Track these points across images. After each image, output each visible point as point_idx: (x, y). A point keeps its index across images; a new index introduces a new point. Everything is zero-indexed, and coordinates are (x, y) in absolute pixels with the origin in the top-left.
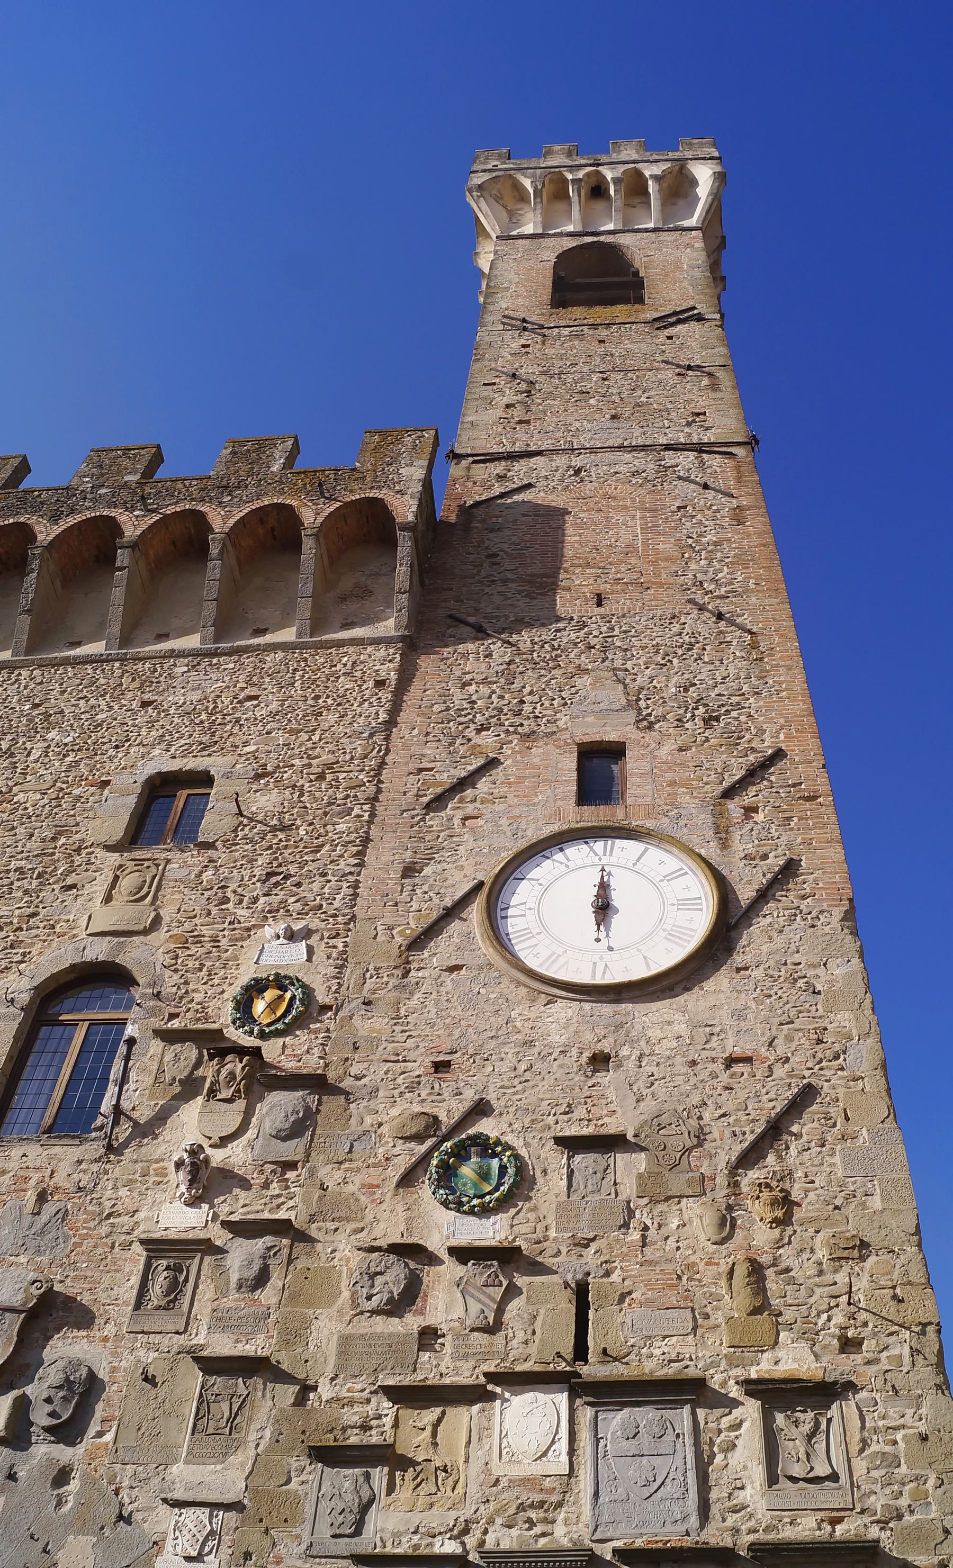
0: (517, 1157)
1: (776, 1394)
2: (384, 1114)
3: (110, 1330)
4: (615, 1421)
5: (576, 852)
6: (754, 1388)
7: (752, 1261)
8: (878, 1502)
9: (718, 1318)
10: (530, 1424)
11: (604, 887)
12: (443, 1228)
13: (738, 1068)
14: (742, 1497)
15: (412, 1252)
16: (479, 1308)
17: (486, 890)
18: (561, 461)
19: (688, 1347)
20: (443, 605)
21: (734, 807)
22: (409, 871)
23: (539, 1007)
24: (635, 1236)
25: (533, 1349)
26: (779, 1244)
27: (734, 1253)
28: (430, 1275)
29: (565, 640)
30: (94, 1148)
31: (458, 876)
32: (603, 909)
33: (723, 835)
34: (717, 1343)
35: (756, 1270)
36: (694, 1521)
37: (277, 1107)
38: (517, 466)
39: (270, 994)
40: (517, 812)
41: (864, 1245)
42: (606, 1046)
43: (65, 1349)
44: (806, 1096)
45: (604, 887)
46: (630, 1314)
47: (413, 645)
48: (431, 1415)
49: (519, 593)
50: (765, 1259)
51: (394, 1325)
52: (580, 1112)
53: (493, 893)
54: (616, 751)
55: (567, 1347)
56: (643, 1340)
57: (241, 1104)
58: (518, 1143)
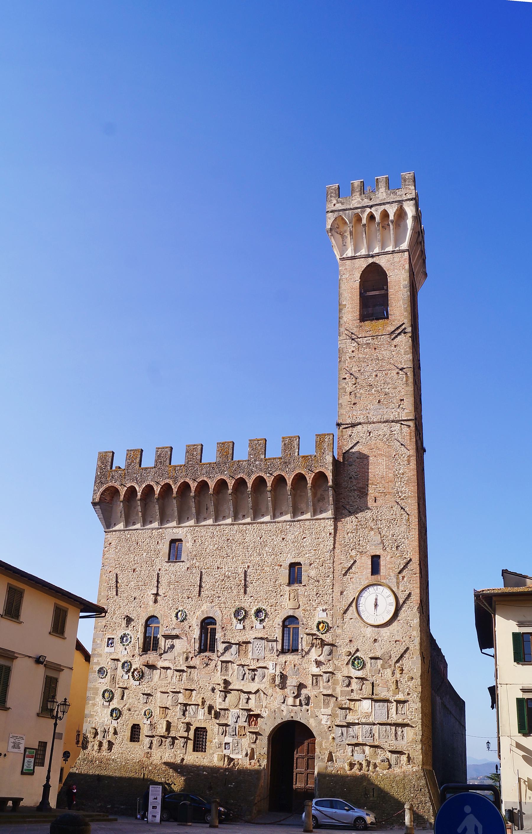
0: (363, 660)
1: (398, 702)
2: (343, 650)
3: (309, 689)
4: (377, 704)
5: (371, 589)
7: (396, 680)
8: (409, 718)
9: (391, 689)
10: (366, 704)
11: (376, 599)
13: (397, 642)
14: (393, 716)
16: (359, 687)
19: (387, 693)
21: (400, 576)
22: (342, 593)
23: (365, 628)
24: (380, 675)
26: (400, 677)
28: (352, 680)
30: (300, 657)
32: (376, 605)
33: (398, 583)
34: (391, 693)
35: (397, 681)
37: (327, 648)
38: (355, 430)
39: (322, 625)
40: (360, 577)
41: (412, 678)
42: (376, 638)
43: (304, 692)
44: (408, 649)
45: (376, 599)
46: (379, 688)
47: (336, 519)
48: (354, 702)
49: (358, 495)
50: (398, 680)
51: (347, 689)
52: (372, 651)
53: (356, 600)
54: (378, 557)
55: (371, 694)
57: (321, 648)
58: (363, 657)
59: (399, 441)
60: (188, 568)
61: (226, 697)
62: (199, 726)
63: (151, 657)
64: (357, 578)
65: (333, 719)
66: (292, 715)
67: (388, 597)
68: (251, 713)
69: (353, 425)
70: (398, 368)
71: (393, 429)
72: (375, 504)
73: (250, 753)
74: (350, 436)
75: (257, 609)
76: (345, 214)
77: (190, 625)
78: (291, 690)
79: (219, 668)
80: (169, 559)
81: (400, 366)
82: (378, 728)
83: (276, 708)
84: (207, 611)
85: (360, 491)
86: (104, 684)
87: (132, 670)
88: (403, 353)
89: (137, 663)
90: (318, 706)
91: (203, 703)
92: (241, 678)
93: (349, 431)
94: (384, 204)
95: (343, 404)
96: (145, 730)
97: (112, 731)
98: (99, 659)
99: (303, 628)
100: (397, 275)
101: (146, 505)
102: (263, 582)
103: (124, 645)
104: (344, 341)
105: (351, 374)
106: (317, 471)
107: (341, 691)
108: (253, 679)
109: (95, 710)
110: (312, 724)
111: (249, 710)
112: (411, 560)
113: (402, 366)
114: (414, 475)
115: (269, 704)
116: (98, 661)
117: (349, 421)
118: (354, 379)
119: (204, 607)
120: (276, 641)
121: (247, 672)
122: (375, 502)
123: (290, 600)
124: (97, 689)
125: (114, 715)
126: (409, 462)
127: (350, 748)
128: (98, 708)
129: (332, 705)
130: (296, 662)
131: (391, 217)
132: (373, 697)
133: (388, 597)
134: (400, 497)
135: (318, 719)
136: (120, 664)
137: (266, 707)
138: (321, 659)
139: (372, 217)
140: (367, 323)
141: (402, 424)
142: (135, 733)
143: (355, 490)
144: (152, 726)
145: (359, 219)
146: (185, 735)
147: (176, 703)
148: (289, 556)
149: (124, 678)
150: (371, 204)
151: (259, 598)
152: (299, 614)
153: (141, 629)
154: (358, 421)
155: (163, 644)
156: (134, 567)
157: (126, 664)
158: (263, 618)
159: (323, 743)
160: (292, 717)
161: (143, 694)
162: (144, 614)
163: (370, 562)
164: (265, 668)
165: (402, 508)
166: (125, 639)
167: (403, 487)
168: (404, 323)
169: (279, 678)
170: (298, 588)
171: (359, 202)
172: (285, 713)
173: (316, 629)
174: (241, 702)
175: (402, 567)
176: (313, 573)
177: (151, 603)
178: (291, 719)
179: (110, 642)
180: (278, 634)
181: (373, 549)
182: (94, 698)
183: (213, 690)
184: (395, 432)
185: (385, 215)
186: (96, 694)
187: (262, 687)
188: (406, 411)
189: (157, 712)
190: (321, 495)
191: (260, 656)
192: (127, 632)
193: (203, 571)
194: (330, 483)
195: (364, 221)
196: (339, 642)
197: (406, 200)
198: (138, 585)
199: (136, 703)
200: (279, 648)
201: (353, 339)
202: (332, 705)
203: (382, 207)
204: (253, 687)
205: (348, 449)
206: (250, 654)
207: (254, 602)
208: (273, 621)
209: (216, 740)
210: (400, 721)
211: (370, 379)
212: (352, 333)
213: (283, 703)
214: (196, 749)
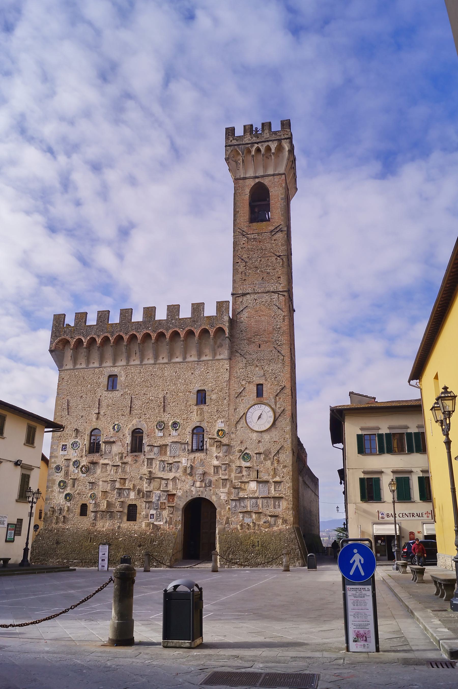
6: (273, 482)
10: (253, 485)
12: (244, 464)
13: (275, 443)
18: (253, 296)
22: (235, 409)
27: (273, 467)
33: (276, 403)
34: (271, 477)
38: (245, 298)
39: (221, 432)
51: (239, 475)
54: (262, 385)
59: (277, 306)
61: (150, 482)
62: (131, 503)
63: (95, 457)
64: (246, 399)
66: (199, 493)
67: (268, 412)
68: (170, 493)
69: (244, 295)
70: (276, 255)
71: (273, 297)
72: (259, 349)
74: (242, 302)
76: (239, 148)
79: (146, 463)
80: (107, 389)
81: (278, 254)
82: (261, 500)
83: (187, 489)
85: (248, 340)
86: (59, 477)
88: (280, 245)
89: (84, 462)
90: (217, 487)
92: (162, 469)
94: (268, 141)
95: (236, 280)
96: (91, 508)
97: (66, 508)
98: (56, 459)
99: (207, 434)
103: (74, 449)
105: (242, 259)
106: (218, 327)
108: (171, 470)
109: (53, 495)
110: (214, 499)
111: (168, 491)
112: (285, 386)
113: (279, 254)
114: (287, 329)
117: (240, 292)
118: (244, 263)
119: (134, 422)
120: (187, 443)
121: (166, 465)
123: (197, 415)
124: (55, 480)
125: (68, 498)
126: (284, 320)
127: (241, 515)
128: (56, 494)
129: (228, 486)
131: (273, 151)
133: (268, 412)
135: (219, 496)
136: (71, 463)
137: (180, 489)
138: (221, 454)
139: (258, 150)
140: (254, 224)
141: (279, 294)
142: (84, 510)
143: (244, 339)
144: (96, 505)
145: (249, 152)
146: (121, 510)
147: (114, 489)
149: (74, 472)
150: (258, 141)
152: (204, 425)
153: (87, 438)
154: (247, 292)
155: (104, 448)
156: (82, 395)
159: (222, 512)
160: (199, 495)
161: (89, 483)
162: (89, 428)
163: (255, 389)
164: (179, 462)
165: (279, 352)
166: (75, 445)
167: (279, 337)
170: (203, 407)
171: (249, 140)
173: (216, 435)
174: (162, 486)
176: (214, 397)
177: (94, 420)
178: (199, 496)
179: (64, 448)
180: (188, 438)
181: (258, 380)
182: (52, 487)
183: (141, 478)
184: (274, 300)
185: (268, 149)
186: (54, 484)
187: (177, 475)
188: (282, 285)
191: (176, 454)
192: (76, 440)
193: (133, 396)
194: (227, 335)
195: (253, 153)
196: (233, 443)
197: (284, 139)
200: (190, 448)
201: (243, 235)
202: (228, 486)
203: (267, 144)
204: (171, 475)
206: (169, 453)
209: (144, 513)
210: (277, 495)
213: (193, 486)
214: (128, 520)
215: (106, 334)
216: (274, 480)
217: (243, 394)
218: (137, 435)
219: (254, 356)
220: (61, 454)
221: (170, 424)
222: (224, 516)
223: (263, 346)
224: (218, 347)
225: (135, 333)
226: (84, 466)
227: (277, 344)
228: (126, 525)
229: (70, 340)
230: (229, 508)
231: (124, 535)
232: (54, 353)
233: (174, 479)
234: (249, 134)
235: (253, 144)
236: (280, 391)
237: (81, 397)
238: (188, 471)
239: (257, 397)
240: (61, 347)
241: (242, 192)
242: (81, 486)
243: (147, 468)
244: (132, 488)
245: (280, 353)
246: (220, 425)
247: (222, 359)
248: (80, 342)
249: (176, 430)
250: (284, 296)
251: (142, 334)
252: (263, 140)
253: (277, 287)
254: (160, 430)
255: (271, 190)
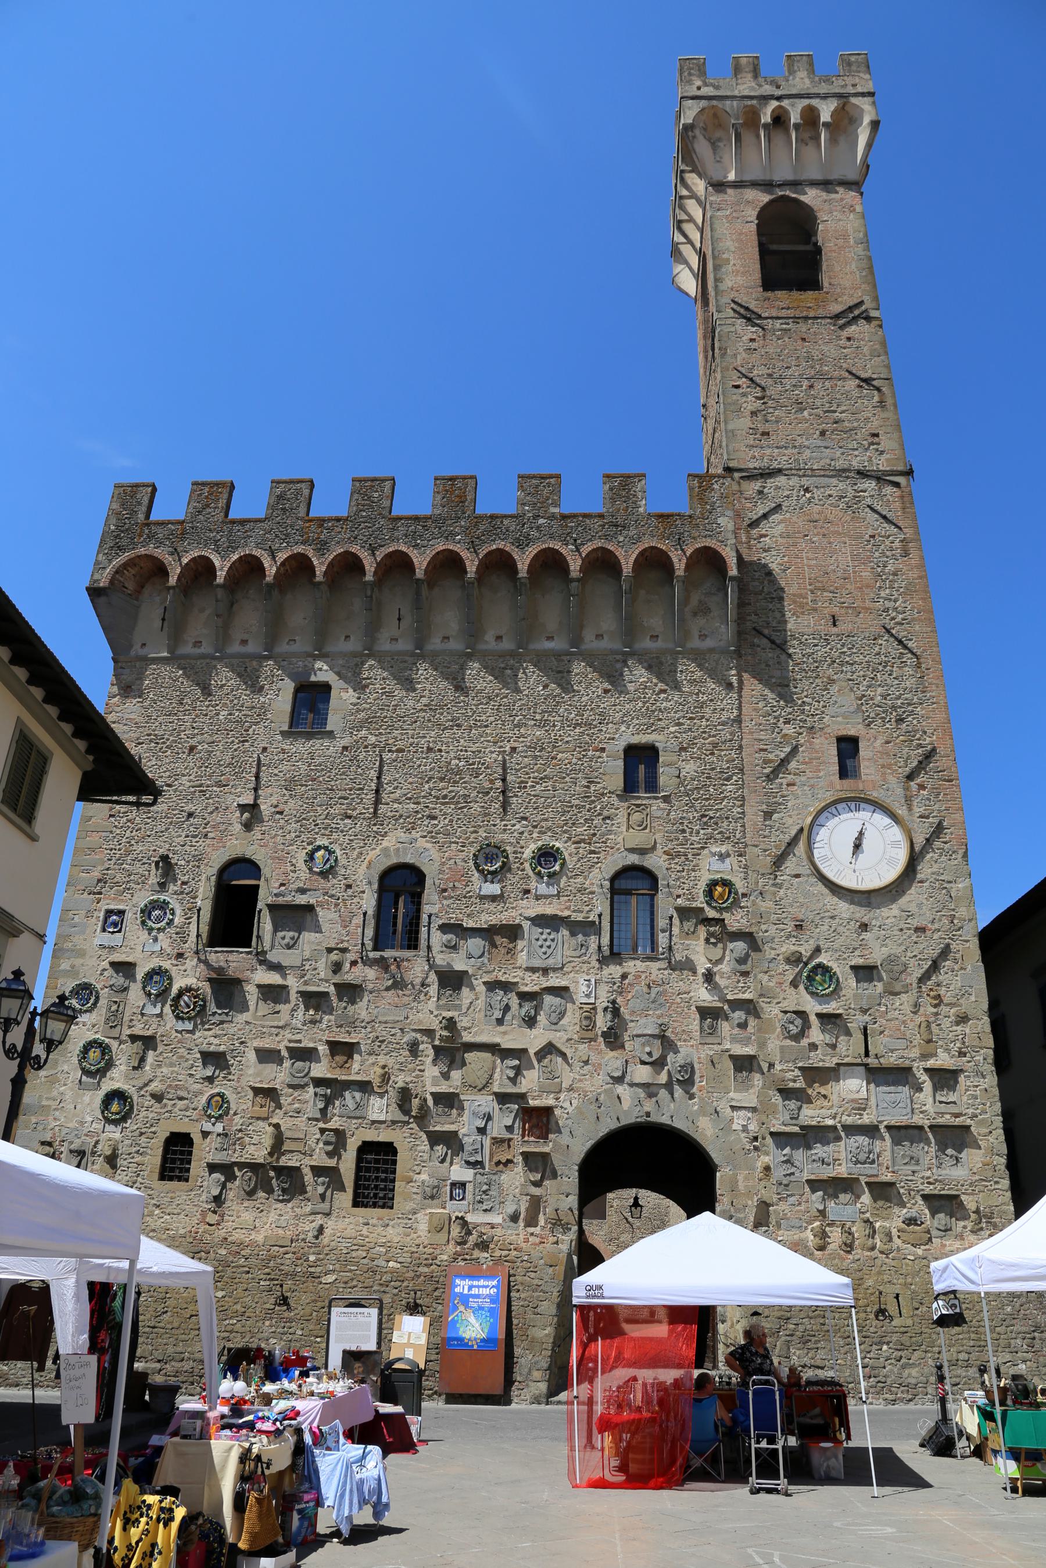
8: (970, 1111)
9: (915, 1042)
12: (812, 1007)
15: (802, 1014)
17: (805, 832)
18: (794, 481)
20: (749, 618)
22: (768, 815)
25: (850, 1052)
29: (820, 653)
31: (790, 821)
32: (857, 846)
33: (908, 800)
34: (915, 1053)
36: (909, 1116)
38: (770, 482)
40: (812, 782)
42: (865, 920)
46: (884, 1039)
56: (889, 1051)
60: (345, 748)
63: (233, 960)
65: (764, 1118)
70: (858, 378)
71: (862, 487)
72: (835, 630)
73: (527, 1210)
74: (760, 492)
75: (540, 849)
77: (350, 882)
78: (643, 1045)
80: (291, 727)
84: (398, 849)
87: (174, 991)
89: (188, 976)
91: (385, 1078)
93: (756, 485)
94: (808, 96)
96: (205, 1152)
98: (78, 962)
100: (840, 220)
101: (232, 605)
102: (554, 787)
103: (151, 930)
104: (729, 321)
107: (782, 1047)
109: (55, 1093)
110: (705, 1131)
111: (522, 1097)
112: (934, 750)
115: (581, 1080)
116: (73, 966)
121: (514, 1001)
122: (835, 625)
123: (629, 827)
125: (115, 1107)
126: (906, 553)
130: (653, 977)
132: (869, 1060)
134: (893, 619)
137: (571, 1089)
139: (779, 120)
148: (623, 728)
151: (543, 824)
152: (656, 862)
154: (775, 465)
157: (156, 978)
158: (557, 868)
159: (740, 1178)
160: (648, 1114)
163: (834, 751)
164: (566, 989)
168: (862, 303)
169: (609, 1016)
172: (626, 1104)
173: (702, 899)
174: (496, 1076)
175: (915, 763)
176: (689, 768)
177: (238, 827)
179: (114, 920)
181: (840, 723)
184: (866, 494)
185: (811, 117)
187: (559, 1039)
188: (885, 456)
189: (242, 1104)
190: (700, 601)
192: (162, 898)
193: (387, 756)
196: (767, 931)
198: (201, 785)
199: (180, 1077)
204: (533, 1040)
205: (755, 517)
207: (531, 833)
208: (585, 879)
209: (424, 1177)
211: (797, 392)
212: (747, 309)
215: (299, 549)
216: (931, 1063)
217: (793, 765)
218: (402, 884)
219: (821, 652)
220: (97, 941)
221: (528, 853)
222: (749, 1194)
223: (843, 627)
224: (695, 614)
225: (404, 549)
226: (189, 989)
227: (893, 619)
228: (347, 1224)
229: (168, 560)
230: (767, 1169)
231: (345, 1261)
232: (102, 600)
233: (549, 1049)
234: (750, 76)
235: (765, 99)
236: (920, 762)
237: (192, 749)
238: (602, 1022)
239: (840, 778)
240: (131, 586)
241: (734, 214)
242: (172, 1065)
243: (438, 1007)
244: (376, 1082)
245: (905, 647)
246: (711, 866)
247: (711, 650)
248: (202, 569)
249: (550, 876)
250: (897, 485)
251: (430, 554)
252: (794, 92)
253: (870, 459)
254: (490, 872)
255: (822, 216)
